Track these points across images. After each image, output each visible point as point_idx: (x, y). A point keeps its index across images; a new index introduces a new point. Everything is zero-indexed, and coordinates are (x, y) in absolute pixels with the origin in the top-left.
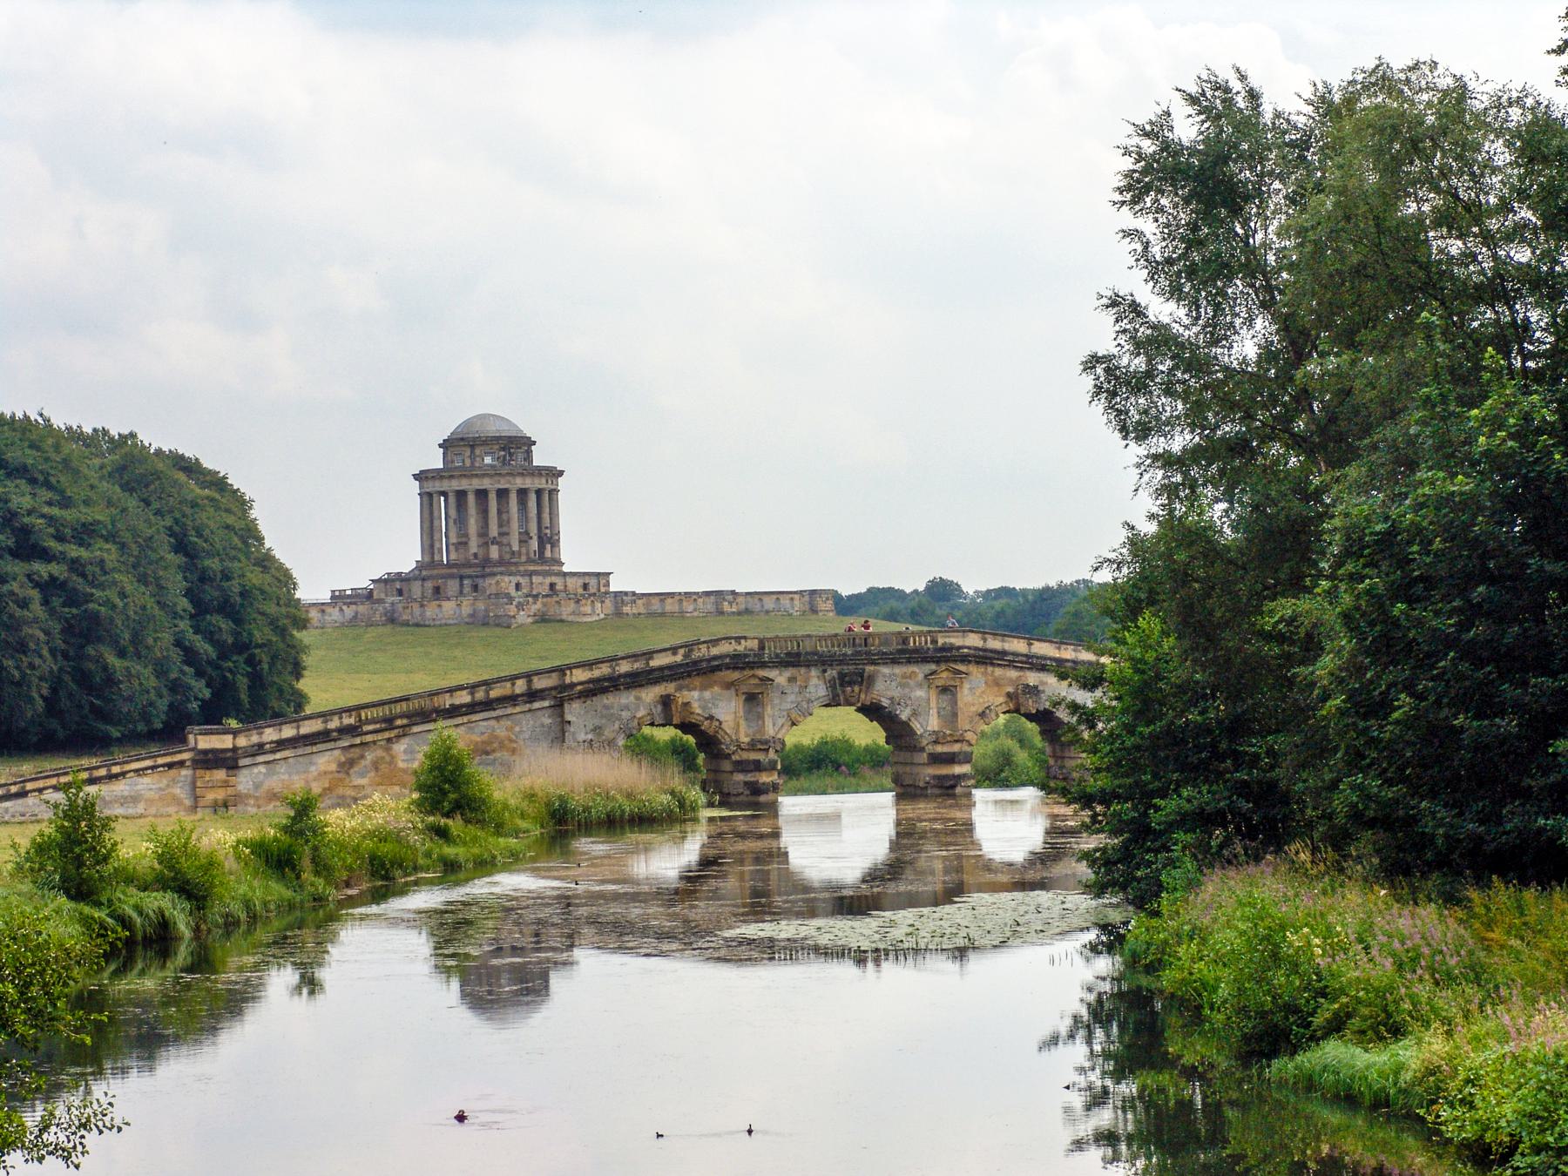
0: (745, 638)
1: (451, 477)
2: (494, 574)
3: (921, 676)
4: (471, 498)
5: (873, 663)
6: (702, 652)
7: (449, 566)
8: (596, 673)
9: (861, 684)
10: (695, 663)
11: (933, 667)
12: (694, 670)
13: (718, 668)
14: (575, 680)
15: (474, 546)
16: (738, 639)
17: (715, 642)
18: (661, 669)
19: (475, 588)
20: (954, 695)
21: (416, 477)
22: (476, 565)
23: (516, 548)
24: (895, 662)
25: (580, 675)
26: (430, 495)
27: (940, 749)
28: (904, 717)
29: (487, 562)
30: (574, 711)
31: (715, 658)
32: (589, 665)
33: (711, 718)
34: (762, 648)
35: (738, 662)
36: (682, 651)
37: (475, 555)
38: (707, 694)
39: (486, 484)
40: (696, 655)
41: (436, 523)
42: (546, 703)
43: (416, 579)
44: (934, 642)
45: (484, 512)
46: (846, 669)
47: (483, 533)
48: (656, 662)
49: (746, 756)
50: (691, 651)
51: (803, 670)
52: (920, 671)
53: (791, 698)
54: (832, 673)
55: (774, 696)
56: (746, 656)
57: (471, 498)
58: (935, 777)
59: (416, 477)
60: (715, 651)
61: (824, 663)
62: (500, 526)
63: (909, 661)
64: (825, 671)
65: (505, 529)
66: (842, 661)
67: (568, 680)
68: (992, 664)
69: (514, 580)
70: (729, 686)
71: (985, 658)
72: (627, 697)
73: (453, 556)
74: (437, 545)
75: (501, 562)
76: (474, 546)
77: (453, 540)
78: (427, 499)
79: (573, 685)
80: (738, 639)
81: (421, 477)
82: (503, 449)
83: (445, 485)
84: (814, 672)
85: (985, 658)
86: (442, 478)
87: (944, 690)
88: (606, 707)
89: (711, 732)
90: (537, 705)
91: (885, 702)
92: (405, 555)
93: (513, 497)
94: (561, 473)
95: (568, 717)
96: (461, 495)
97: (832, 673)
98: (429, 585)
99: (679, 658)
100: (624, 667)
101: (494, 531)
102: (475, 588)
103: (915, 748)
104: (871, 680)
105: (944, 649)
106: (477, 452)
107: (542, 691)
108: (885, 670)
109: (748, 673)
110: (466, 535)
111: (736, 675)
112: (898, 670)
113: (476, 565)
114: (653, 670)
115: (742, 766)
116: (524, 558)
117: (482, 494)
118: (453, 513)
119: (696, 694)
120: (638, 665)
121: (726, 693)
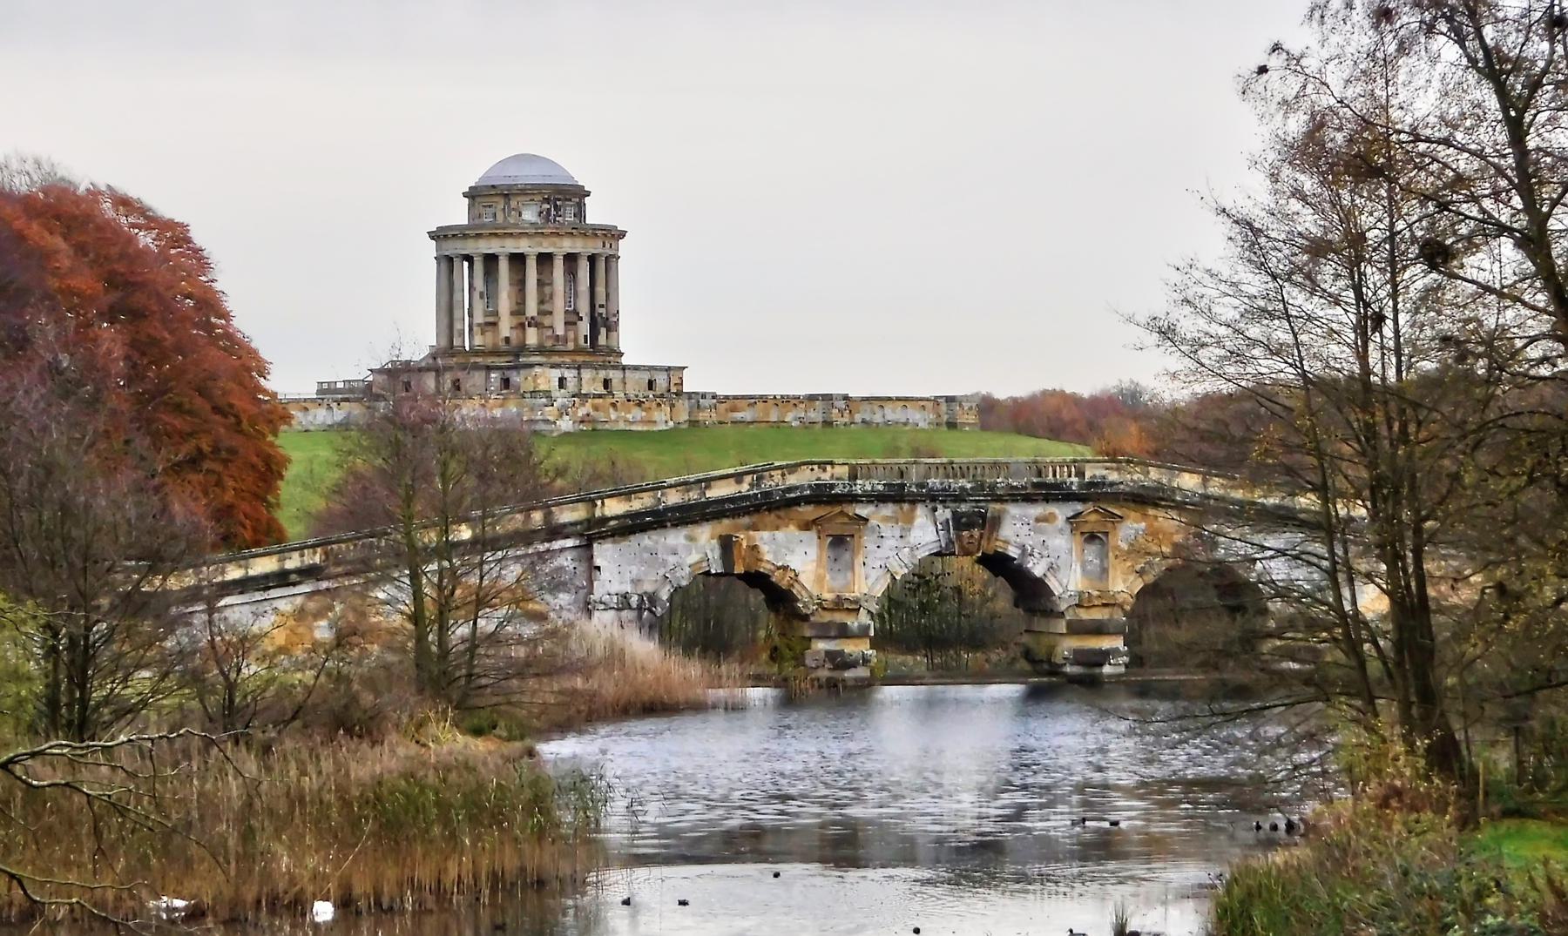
0: (832, 463)
1: (479, 236)
2: (531, 366)
3: (1061, 521)
4: (504, 266)
5: (1000, 499)
6: (774, 482)
7: (475, 352)
8: (636, 505)
9: (983, 526)
10: (767, 494)
11: (1079, 507)
12: (768, 506)
13: (796, 502)
14: (608, 512)
15: (506, 328)
17: (793, 468)
18: (721, 501)
19: (506, 383)
20: (1103, 544)
21: (433, 236)
22: (507, 353)
23: (560, 331)
24: (1029, 499)
25: (614, 507)
26: (450, 260)
27: (1084, 615)
28: (1038, 571)
29: (522, 349)
30: (604, 553)
31: (790, 489)
32: (627, 495)
33: (785, 568)
34: (853, 477)
35: (821, 496)
36: (748, 479)
37: (507, 340)
38: (779, 535)
39: (523, 246)
40: (767, 484)
41: (457, 296)
42: (570, 543)
43: (428, 369)
44: (1080, 474)
45: (520, 284)
46: (964, 508)
47: (518, 310)
48: (718, 491)
49: (827, 617)
50: (760, 479)
51: (906, 506)
52: (1061, 512)
53: (890, 543)
54: (944, 513)
55: (868, 541)
56: (832, 486)
57: (504, 266)
58: (1076, 652)
59: (433, 236)
60: (792, 480)
61: (934, 499)
62: (541, 302)
63: (1047, 499)
64: (935, 510)
65: (546, 307)
66: (959, 497)
67: (598, 513)
68: (1156, 506)
69: (556, 373)
70: (806, 526)
71: (1143, 499)
72: (675, 538)
73: (478, 340)
74: (457, 326)
75: (541, 350)
76: (506, 328)
77: (479, 318)
78: (447, 263)
79: (605, 520)
80: (822, 465)
81: (439, 236)
82: (547, 201)
83: (470, 247)
84: (921, 512)
85: (1143, 499)
86: (465, 236)
87: (1092, 538)
88: (646, 549)
89: (784, 584)
90: (557, 545)
91: (1013, 552)
92: (418, 337)
93: (559, 264)
94: (622, 234)
95: (598, 561)
96: (491, 260)
97: (944, 513)
98: (448, 380)
99: (745, 488)
100: (673, 498)
101: (532, 309)
102: (506, 383)
103: (1053, 614)
104: (996, 522)
105: (1092, 484)
106: (513, 204)
107: (564, 525)
108: (1014, 510)
109: (838, 509)
110: (496, 313)
111: (822, 511)
112: (1037, 510)
113: (507, 353)
114: (710, 503)
115: (825, 632)
117: (518, 260)
118: (479, 284)
119: (766, 534)
120: (694, 495)
121: (806, 535)
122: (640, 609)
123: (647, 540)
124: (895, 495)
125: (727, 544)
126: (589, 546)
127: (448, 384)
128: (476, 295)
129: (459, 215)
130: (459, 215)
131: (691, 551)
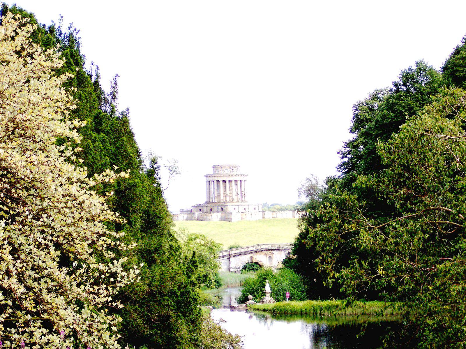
1: (215, 176)
4: (221, 183)
16: (267, 244)
21: (206, 176)
34: (272, 246)
36: (255, 247)
39: (225, 179)
40: (258, 248)
42: (226, 258)
48: (250, 249)
57: (221, 183)
61: (285, 250)
74: (211, 197)
77: (216, 195)
81: (206, 176)
84: (283, 252)
90: (224, 258)
93: (233, 182)
96: (218, 181)
100: (243, 250)
102: (222, 209)
110: (219, 193)
116: (236, 201)
118: (216, 187)
122: (238, 268)
123: (239, 257)
124: (278, 249)
125: (251, 258)
126: (229, 258)
127: (209, 210)
128: (215, 190)
129: (211, 171)
130: (211, 171)
131: (245, 259)
